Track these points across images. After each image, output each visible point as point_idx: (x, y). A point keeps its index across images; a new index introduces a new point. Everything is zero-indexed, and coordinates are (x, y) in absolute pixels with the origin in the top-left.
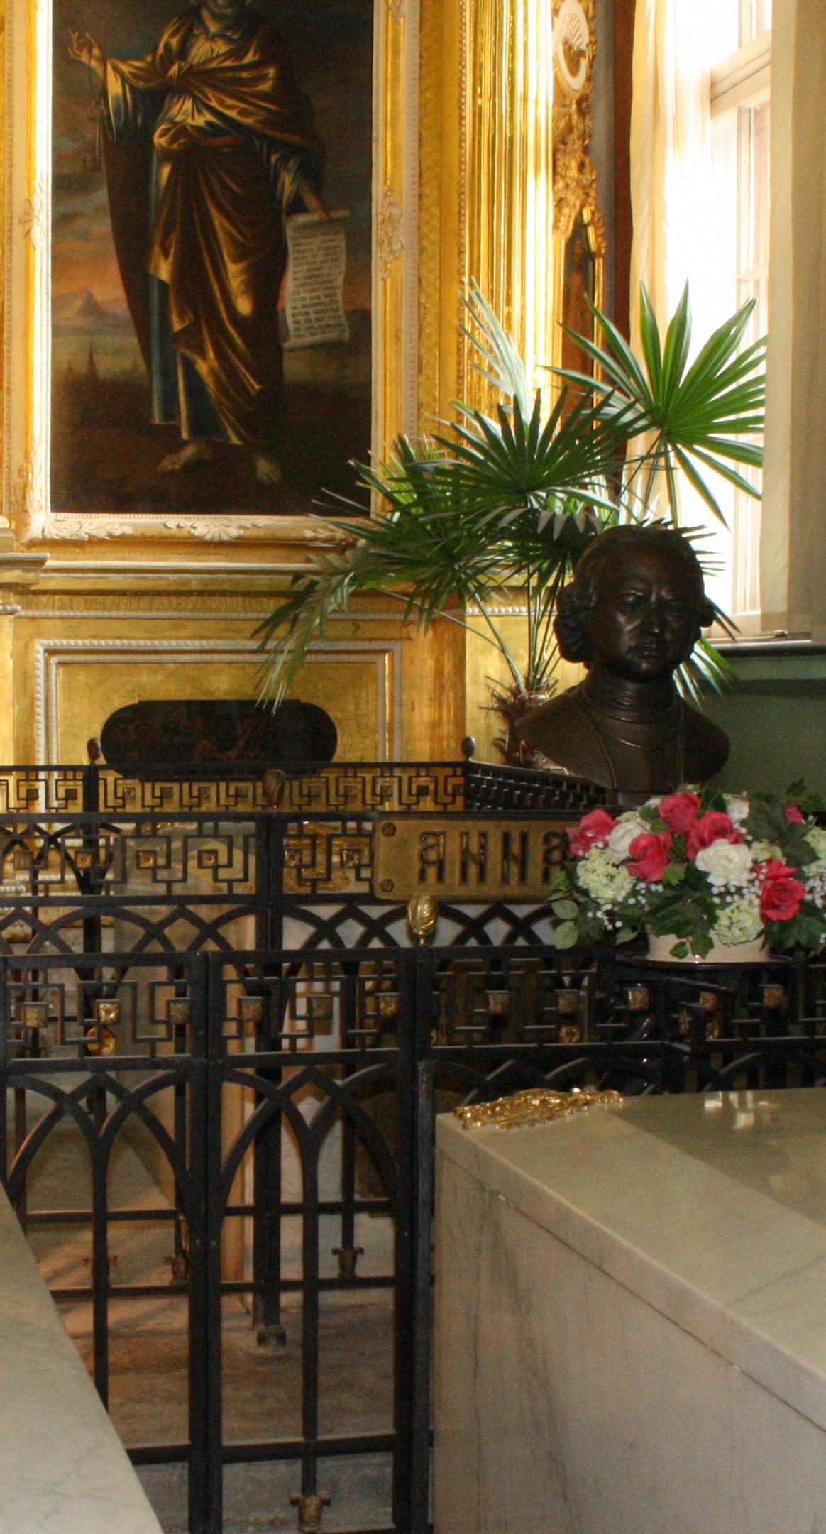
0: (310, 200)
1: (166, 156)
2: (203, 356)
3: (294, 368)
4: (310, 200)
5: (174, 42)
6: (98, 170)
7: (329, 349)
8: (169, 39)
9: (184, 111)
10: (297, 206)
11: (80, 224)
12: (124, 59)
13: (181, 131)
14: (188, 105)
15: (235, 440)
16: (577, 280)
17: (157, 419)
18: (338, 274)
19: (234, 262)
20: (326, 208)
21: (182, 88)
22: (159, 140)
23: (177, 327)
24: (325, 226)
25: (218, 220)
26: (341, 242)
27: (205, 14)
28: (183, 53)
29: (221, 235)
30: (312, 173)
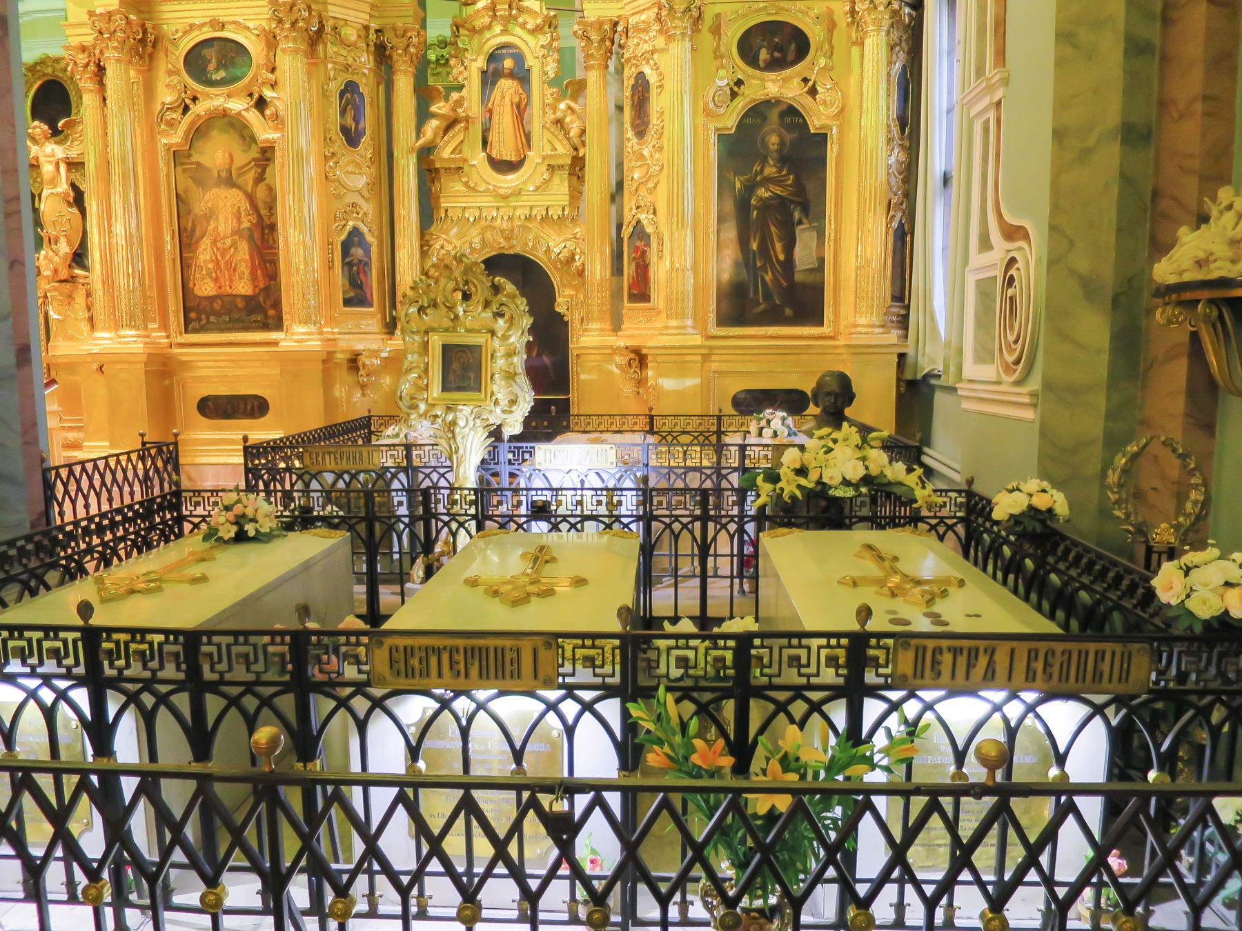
0: (805, 220)
1: (756, 208)
2: (767, 274)
3: (798, 277)
4: (805, 220)
7: (811, 270)
8: (757, 167)
9: (762, 192)
10: (800, 222)
12: (743, 175)
13: (761, 199)
15: (778, 302)
16: (899, 243)
17: (752, 295)
18: (814, 244)
19: (779, 242)
22: (753, 202)
23: (759, 265)
24: (811, 228)
25: (773, 229)
26: (815, 234)
28: (762, 171)
30: (805, 210)
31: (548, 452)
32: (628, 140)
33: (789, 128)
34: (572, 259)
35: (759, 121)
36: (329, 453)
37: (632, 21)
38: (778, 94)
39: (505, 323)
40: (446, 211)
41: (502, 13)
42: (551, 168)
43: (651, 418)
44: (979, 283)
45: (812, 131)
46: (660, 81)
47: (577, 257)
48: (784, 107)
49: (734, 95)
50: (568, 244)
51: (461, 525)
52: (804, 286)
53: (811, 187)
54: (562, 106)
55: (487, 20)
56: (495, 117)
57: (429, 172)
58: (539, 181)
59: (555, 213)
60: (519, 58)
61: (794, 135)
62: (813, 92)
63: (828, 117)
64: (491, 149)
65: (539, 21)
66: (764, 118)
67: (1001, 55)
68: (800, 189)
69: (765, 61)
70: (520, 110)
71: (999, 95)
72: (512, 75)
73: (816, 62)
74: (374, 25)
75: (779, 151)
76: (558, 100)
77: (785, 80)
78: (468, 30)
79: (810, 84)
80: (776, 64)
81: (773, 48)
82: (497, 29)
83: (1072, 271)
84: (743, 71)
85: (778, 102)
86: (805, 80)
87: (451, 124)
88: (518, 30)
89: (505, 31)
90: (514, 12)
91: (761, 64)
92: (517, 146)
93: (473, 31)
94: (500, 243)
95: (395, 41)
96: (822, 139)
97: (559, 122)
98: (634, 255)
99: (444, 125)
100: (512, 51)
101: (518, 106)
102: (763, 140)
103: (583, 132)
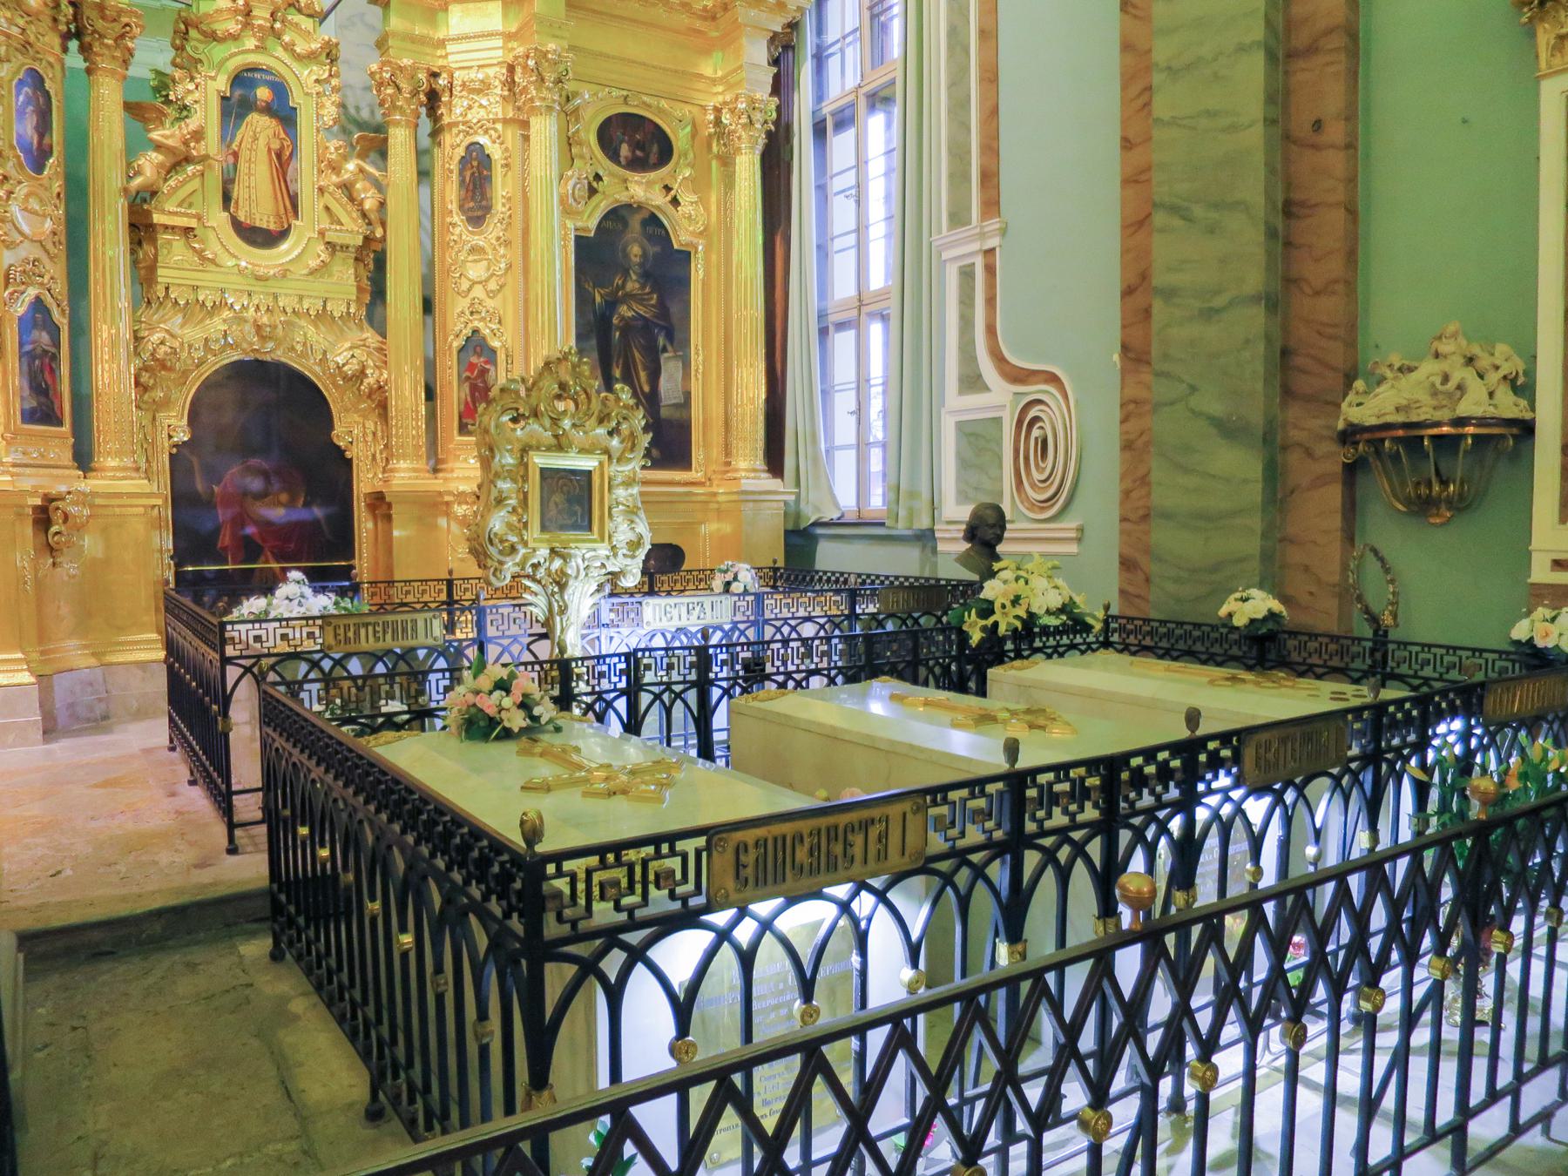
0: (669, 348)
1: (618, 328)
4: (669, 348)
7: (676, 406)
8: (618, 281)
9: (624, 310)
10: (665, 350)
12: (602, 288)
13: (622, 318)
20: (675, 351)
22: (615, 321)
24: (676, 357)
25: (637, 355)
30: (670, 336)
32: (454, 225)
33: (651, 238)
34: (361, 374)
35: (620, 226)
36: (366, 625)
37: (459, 76)
38: (643, 199)
39: (622, 442)
41: (260, 22)
42: (332, 247)
43: (450, 583)
44: (960, 426)
45: (676, 247)
46: (506, 159)
47: (369, 372)
49: (592, 191)
50: (357, 352)
51: (678, 695)
52: (669, 422)
53: (674, 309)
54: (351, 166)
55: (233, 26)
56: (243, 166)
57: (141, 229)
58: (313, 263)
59: (337, 309)
60: (280, 90)
61: (657, 249)
62: (675, 202)
63: (693, 233)
65: (315, 46)
66: (625, 224)
67: (991, 205)
68: (663, 310)
69: (626, 158)
70: (282, 162)
71: (993, 242)
72: (268, 110)
73: (680, 172)
75: (642, 265)
76: (345, 158)
77: (650, 184)
78: (204, 33)
79: (673, 193)
80: (638, 164)
82: (250, 43)
83: (1197, 414)
84: (605, 165)
85: (640, 207)
86: (668, 189)
87: (179, 161)
88: (280, 52)
89: (260, 49)
90: (278, 25)
91: (622, 160)
92: (278, 211)
93: (212, 37)
94: (252, 344)
95: (100, 24)
96: (685, 257)
97: (347, 187)
98: (468, 374)
99: (172, 160)
100: (268, 78)
101: (279, 156)
102: (624, 250)
103: (382, 204)
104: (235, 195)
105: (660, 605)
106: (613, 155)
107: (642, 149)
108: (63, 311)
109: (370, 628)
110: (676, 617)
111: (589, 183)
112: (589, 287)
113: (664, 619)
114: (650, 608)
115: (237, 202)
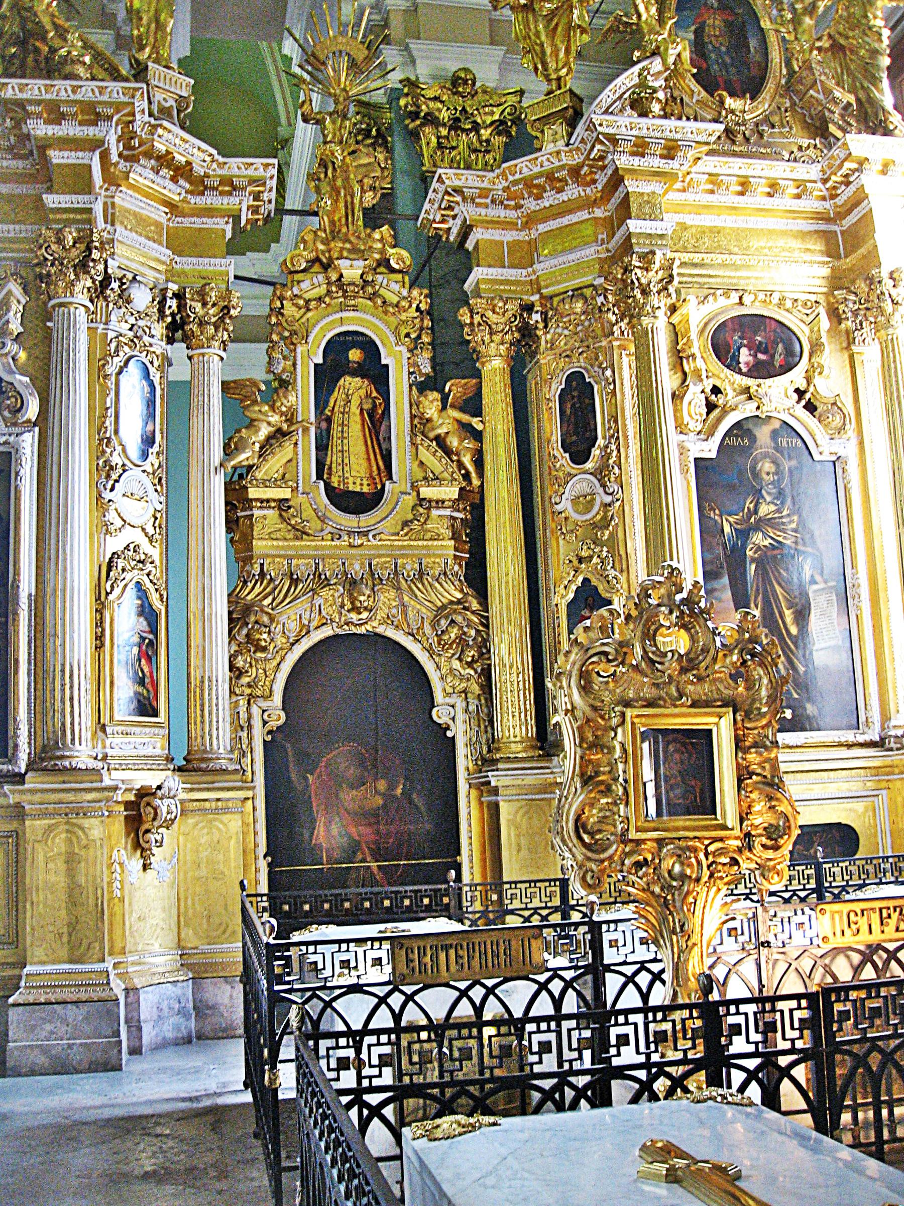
0: (818, 578)
1: (753, 560)
5: (752, 506)
6: (722, 567)
9: (758, 539)
11: (716, 594)
14: (760, 534)
15: (796, 696)
20: (826, 582)
21: (757, 528)
22: (749, 553)
26: (834, 597)
27: (764, 492)
28: (756, 512)
29: (780, 597)
31: (837, 916)
36: (446, 948)
40: (262, 565)
48: (777, 425)
49: (711, 407)
60: (370, 348)
64: (330, 474)
66: (753, 439)
69: (747, 364)
72: (359, 371)
74: (173, 287)
79: (808, 396)
81: (756, 349)
91: (744, 370)
92: (371, 474)
101: (371, 415)
102: (753, 468)
104: (328, 463)
105: (840, 912)
106: (733, 365)
107: (765, 352)
108: (161, 595)
109: (452, 952)
110: (864, 929)
111: (707, 398)
112: (715, 515)
113: (848, 932)
114: (828, 914)
115: (330, 468)
